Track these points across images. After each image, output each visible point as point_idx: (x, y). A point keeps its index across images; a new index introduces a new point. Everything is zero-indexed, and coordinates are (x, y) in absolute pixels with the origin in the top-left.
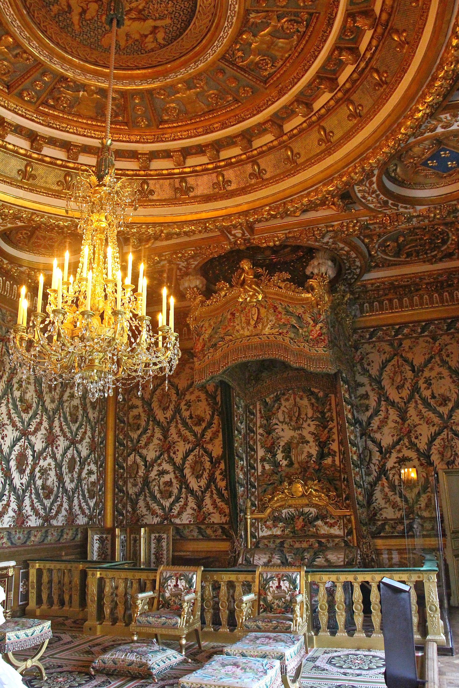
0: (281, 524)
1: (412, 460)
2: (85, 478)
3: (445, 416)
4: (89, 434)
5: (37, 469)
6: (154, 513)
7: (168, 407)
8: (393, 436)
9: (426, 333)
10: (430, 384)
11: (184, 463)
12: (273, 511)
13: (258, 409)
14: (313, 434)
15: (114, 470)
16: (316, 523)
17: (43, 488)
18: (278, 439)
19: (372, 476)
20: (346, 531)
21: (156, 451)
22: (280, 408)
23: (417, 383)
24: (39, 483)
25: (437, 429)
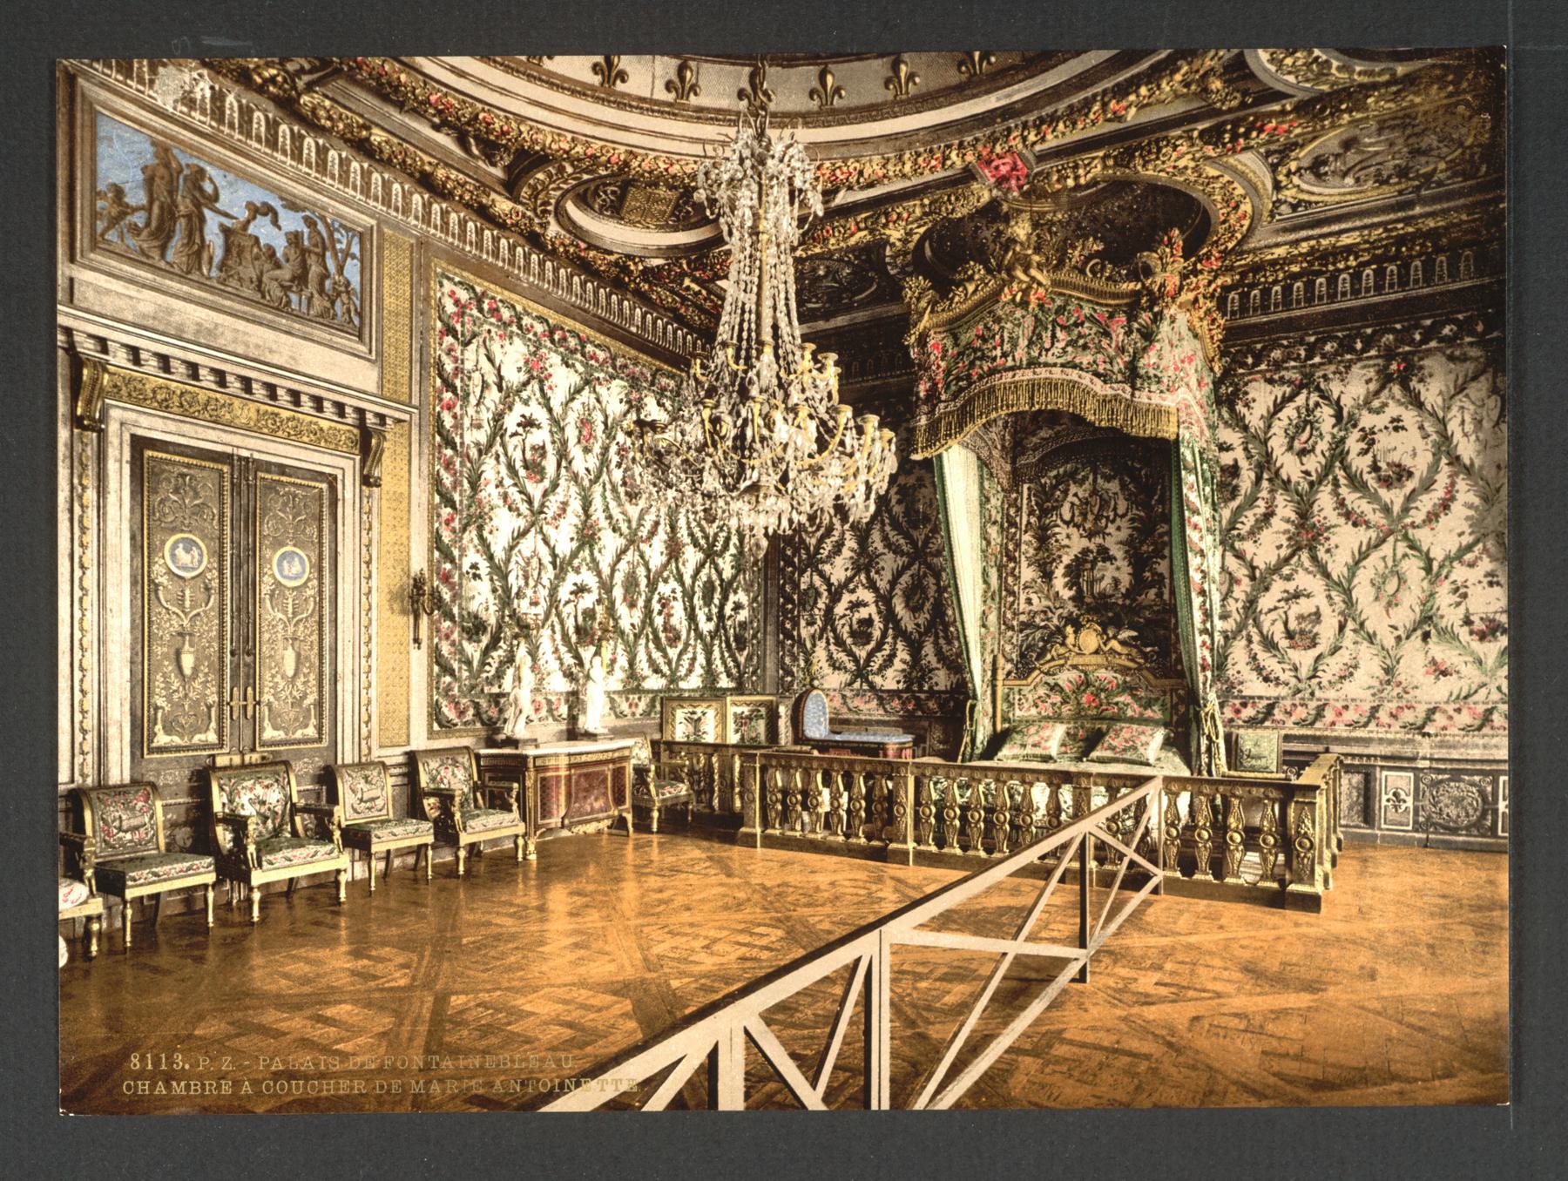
5: (656, 597)
9: (1373, 353)
17: (665, 630)
19: (1231, 620)
24: (659, 621)
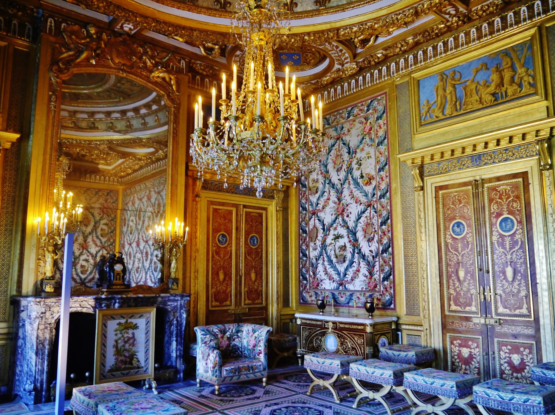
1: (343, 237)
3: (370, 195)
8: (332, 215)
10: (360, 165)
19: (317, 250)
23: (351, 164)
25: (363, 207)
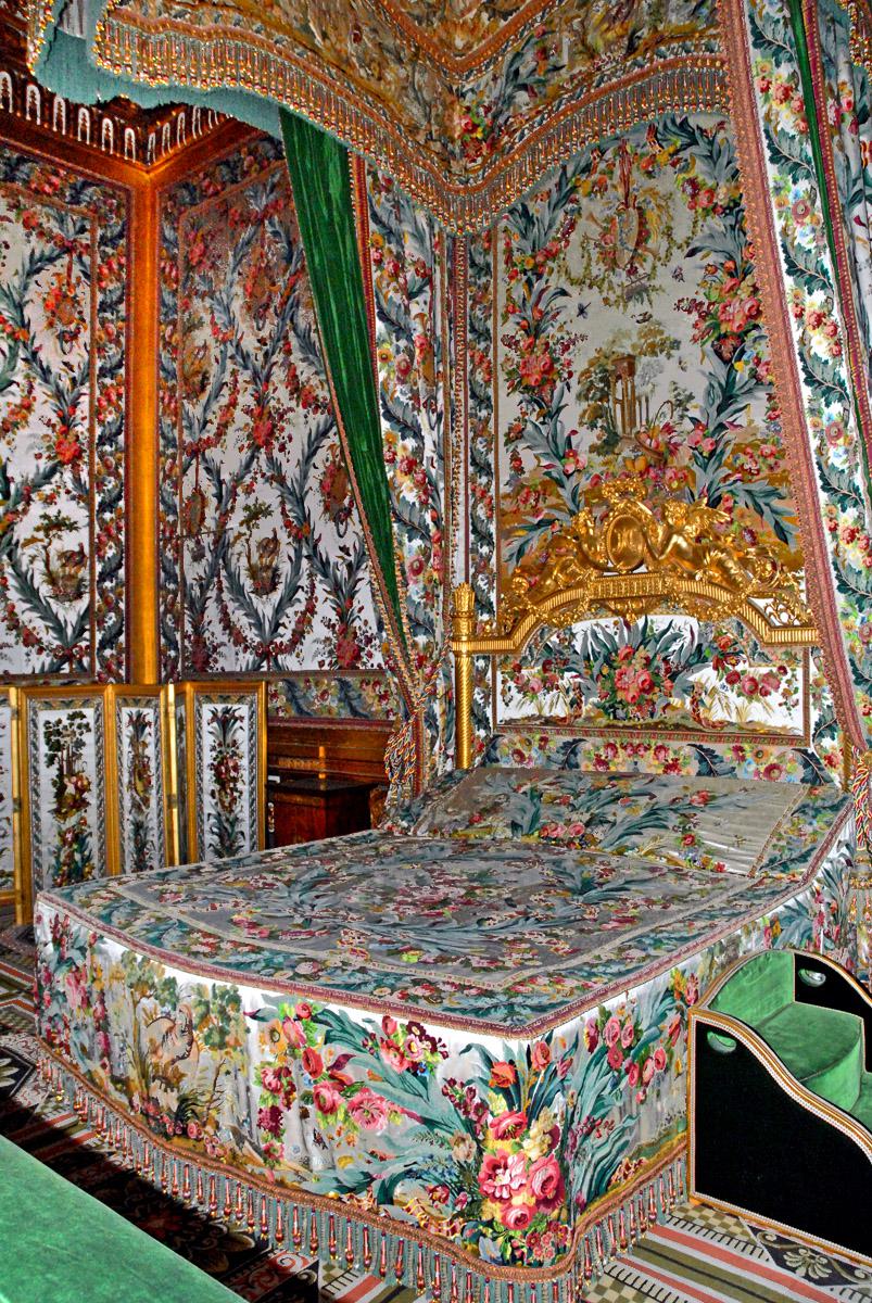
0: (567, 679)
2: (33, 540)
4: (45, 408)
6: (239, 639)
7: (267, 307)
11: (305, 476)
12: (542, 628)
13: (501, 245)
14: (695, 305)
15: (159, 519)
16: (693, 678)
18: (566, 348)
20: (815, 716)
21: (241, 449)
22: (572, 225)
